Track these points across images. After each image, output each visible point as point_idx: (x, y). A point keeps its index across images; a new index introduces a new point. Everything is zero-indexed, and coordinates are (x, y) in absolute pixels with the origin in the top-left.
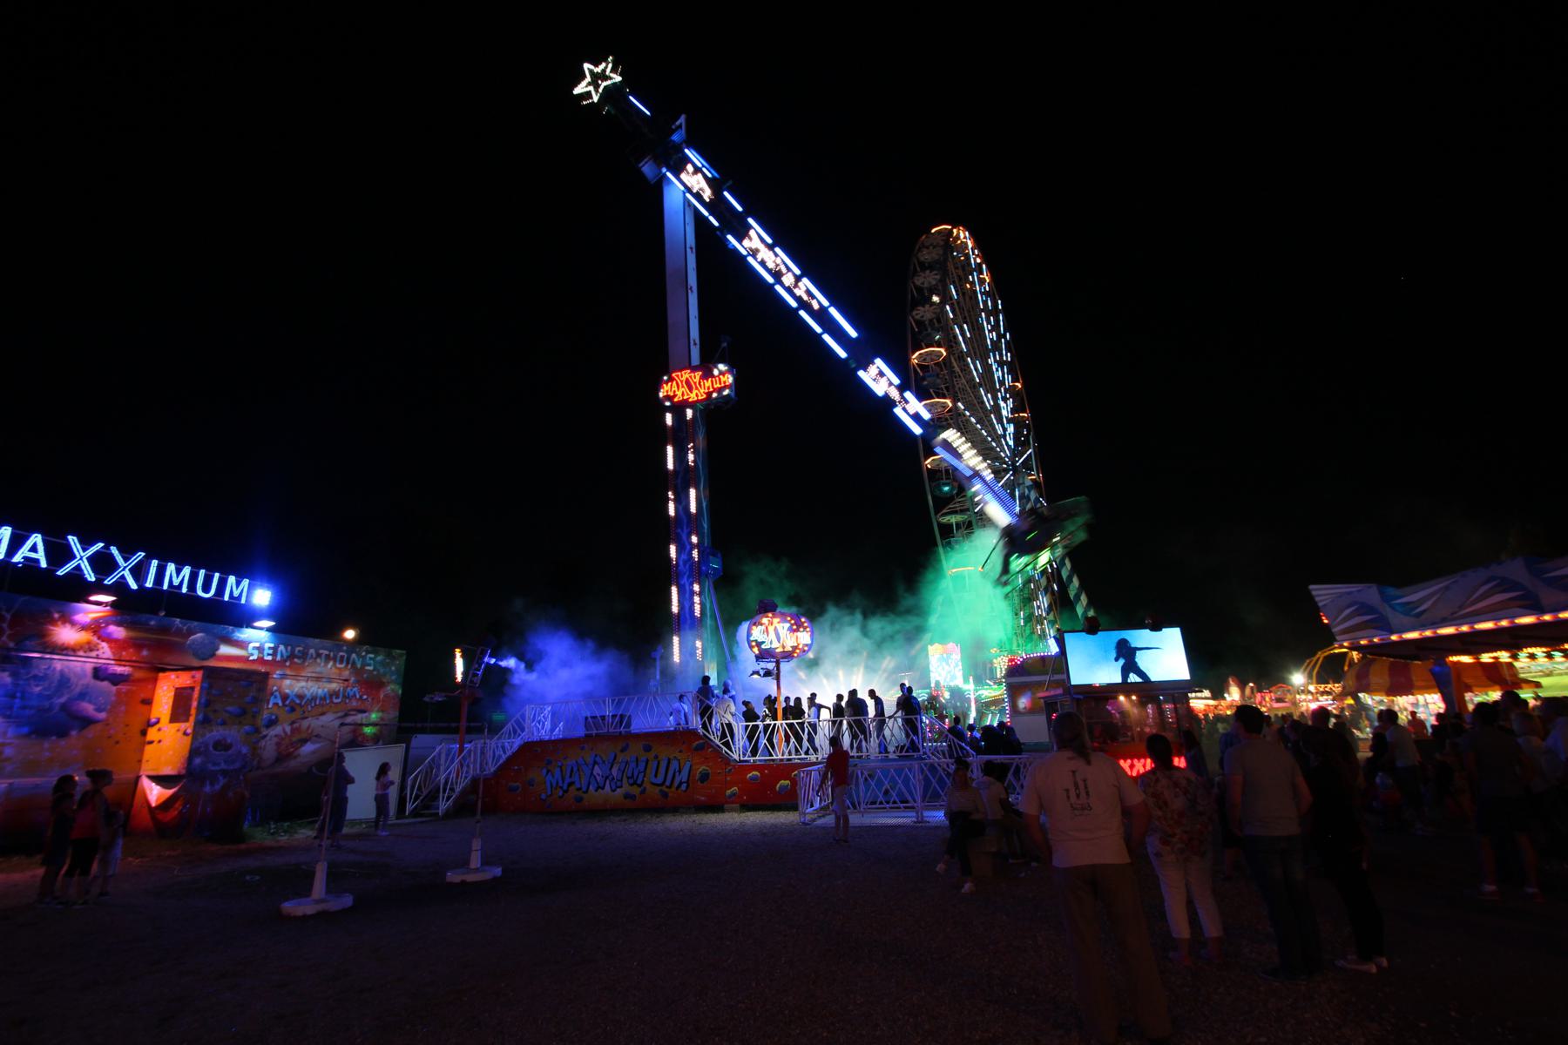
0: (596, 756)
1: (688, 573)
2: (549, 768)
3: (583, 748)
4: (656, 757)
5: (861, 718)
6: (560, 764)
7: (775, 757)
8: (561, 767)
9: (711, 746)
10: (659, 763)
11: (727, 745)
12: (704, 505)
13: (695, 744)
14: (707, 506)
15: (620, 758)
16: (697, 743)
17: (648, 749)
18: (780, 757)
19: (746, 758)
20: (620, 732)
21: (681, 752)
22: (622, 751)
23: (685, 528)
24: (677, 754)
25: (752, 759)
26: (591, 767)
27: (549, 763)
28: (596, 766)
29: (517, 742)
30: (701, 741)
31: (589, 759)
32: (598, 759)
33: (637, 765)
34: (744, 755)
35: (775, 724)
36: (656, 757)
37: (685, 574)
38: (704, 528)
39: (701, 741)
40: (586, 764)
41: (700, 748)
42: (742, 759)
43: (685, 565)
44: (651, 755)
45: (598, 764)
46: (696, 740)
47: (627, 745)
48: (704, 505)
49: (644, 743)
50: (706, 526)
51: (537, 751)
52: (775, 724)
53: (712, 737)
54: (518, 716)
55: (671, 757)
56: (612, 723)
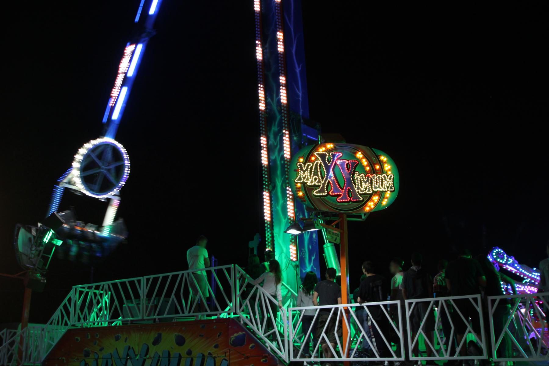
0: (129, 348)
1: (278, 147)
2: (87, 360)
3: (117, 339)
4: (189, 353)
5: (470, 297)
6: (96, 357)
7: (337, 359)
8: (97, 360)
9: (252, 340)
10: (192, 360)
11: (273, 337)
12: (298, 70)
13: (233, 337)
14: (300, 72)
15: (153, 350)
16: (235, 335)
17: (180, 342)
18: (344, 358)
19: (298, 359)
20: (155, 319)
21: (216, 347)
22: (156, 342)
23: (275, 95)
24: (212, 350)
25: (305, 360)
26: (124, 361)
27: (87, 355)
28: (129, 361)
29: (63, 330)
30: (240, 333)
31: (122, 353)
32: (131, 352)
33: (169, 360)
34: (295, 356)
35: (337, 309)
36: (189, 353)
37: (276, 146)
38: (298, 96)
39: (240, 333)
40: (120, 357)
41: (239, 342)
42: (292, 359)
43: (275, 138)
44: (183, 350)
45: (130, 358)
46: (237, 332)
47: (160, 336)
48: (298, 70)
49: (176, 333)
50: (300, 94)
51: (77, 339)
52: (337, 309)
53: (255, 328)
54: (66, 301)
55: (206, 354)
56: (147, 307)
